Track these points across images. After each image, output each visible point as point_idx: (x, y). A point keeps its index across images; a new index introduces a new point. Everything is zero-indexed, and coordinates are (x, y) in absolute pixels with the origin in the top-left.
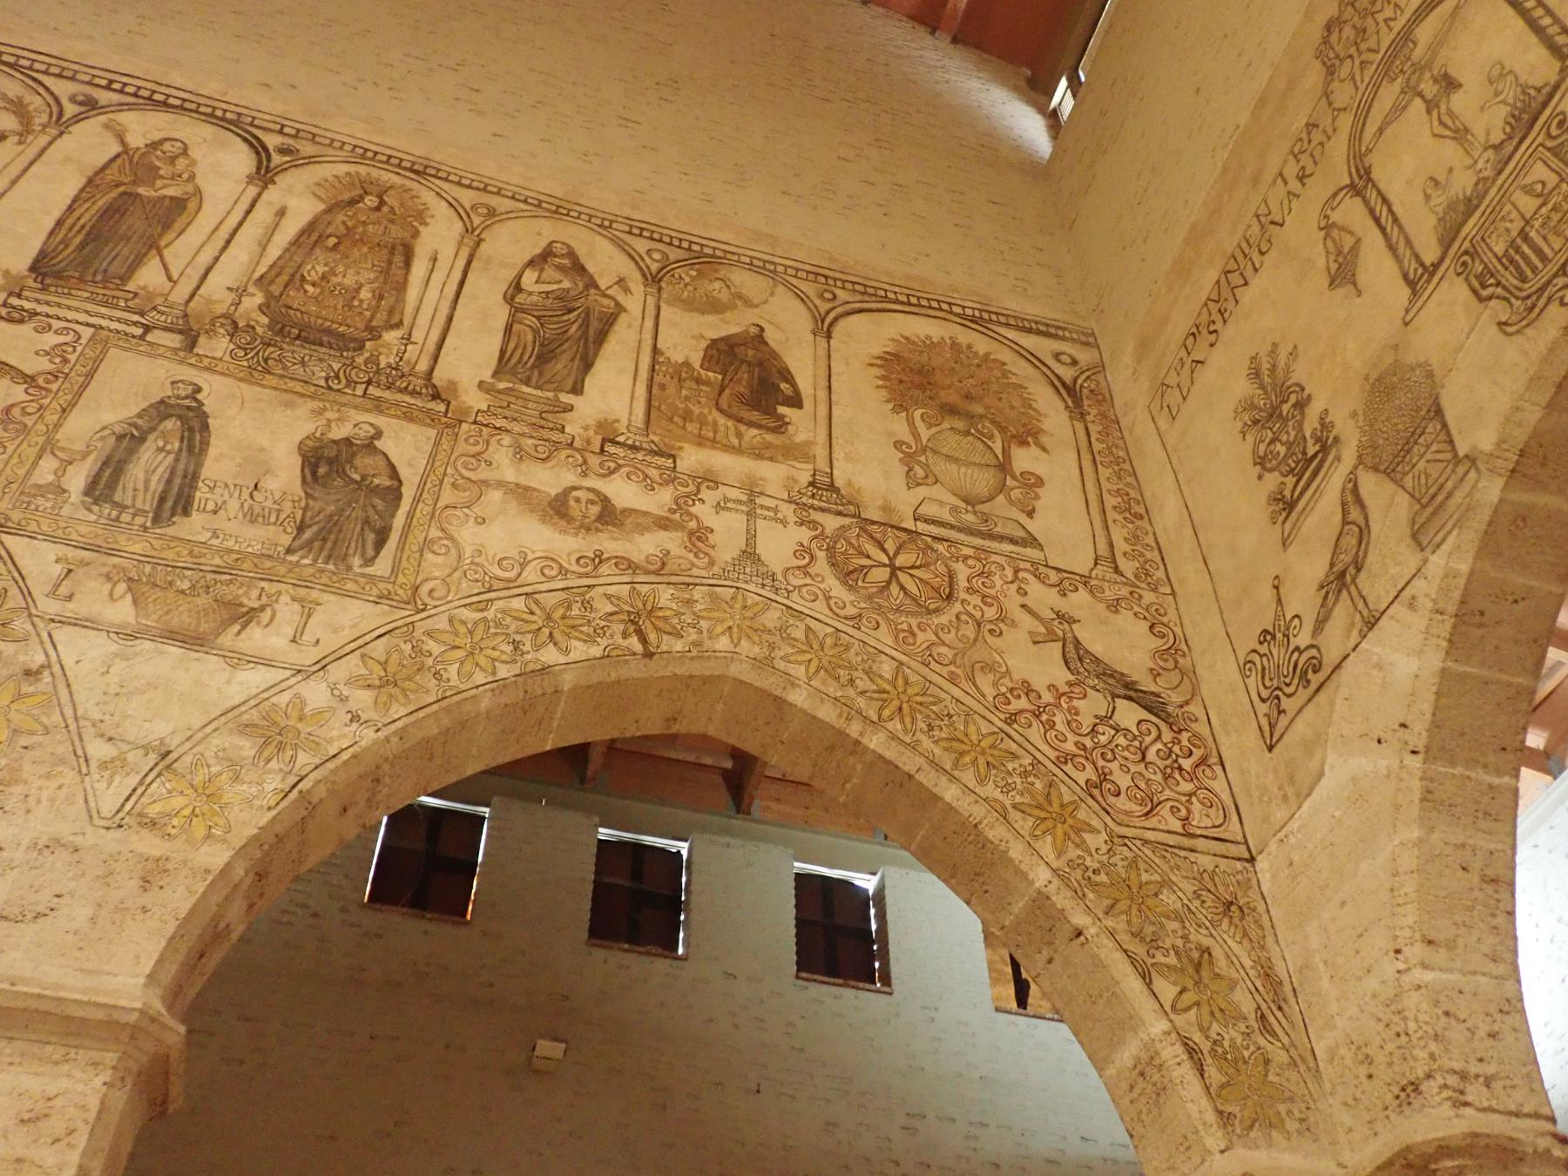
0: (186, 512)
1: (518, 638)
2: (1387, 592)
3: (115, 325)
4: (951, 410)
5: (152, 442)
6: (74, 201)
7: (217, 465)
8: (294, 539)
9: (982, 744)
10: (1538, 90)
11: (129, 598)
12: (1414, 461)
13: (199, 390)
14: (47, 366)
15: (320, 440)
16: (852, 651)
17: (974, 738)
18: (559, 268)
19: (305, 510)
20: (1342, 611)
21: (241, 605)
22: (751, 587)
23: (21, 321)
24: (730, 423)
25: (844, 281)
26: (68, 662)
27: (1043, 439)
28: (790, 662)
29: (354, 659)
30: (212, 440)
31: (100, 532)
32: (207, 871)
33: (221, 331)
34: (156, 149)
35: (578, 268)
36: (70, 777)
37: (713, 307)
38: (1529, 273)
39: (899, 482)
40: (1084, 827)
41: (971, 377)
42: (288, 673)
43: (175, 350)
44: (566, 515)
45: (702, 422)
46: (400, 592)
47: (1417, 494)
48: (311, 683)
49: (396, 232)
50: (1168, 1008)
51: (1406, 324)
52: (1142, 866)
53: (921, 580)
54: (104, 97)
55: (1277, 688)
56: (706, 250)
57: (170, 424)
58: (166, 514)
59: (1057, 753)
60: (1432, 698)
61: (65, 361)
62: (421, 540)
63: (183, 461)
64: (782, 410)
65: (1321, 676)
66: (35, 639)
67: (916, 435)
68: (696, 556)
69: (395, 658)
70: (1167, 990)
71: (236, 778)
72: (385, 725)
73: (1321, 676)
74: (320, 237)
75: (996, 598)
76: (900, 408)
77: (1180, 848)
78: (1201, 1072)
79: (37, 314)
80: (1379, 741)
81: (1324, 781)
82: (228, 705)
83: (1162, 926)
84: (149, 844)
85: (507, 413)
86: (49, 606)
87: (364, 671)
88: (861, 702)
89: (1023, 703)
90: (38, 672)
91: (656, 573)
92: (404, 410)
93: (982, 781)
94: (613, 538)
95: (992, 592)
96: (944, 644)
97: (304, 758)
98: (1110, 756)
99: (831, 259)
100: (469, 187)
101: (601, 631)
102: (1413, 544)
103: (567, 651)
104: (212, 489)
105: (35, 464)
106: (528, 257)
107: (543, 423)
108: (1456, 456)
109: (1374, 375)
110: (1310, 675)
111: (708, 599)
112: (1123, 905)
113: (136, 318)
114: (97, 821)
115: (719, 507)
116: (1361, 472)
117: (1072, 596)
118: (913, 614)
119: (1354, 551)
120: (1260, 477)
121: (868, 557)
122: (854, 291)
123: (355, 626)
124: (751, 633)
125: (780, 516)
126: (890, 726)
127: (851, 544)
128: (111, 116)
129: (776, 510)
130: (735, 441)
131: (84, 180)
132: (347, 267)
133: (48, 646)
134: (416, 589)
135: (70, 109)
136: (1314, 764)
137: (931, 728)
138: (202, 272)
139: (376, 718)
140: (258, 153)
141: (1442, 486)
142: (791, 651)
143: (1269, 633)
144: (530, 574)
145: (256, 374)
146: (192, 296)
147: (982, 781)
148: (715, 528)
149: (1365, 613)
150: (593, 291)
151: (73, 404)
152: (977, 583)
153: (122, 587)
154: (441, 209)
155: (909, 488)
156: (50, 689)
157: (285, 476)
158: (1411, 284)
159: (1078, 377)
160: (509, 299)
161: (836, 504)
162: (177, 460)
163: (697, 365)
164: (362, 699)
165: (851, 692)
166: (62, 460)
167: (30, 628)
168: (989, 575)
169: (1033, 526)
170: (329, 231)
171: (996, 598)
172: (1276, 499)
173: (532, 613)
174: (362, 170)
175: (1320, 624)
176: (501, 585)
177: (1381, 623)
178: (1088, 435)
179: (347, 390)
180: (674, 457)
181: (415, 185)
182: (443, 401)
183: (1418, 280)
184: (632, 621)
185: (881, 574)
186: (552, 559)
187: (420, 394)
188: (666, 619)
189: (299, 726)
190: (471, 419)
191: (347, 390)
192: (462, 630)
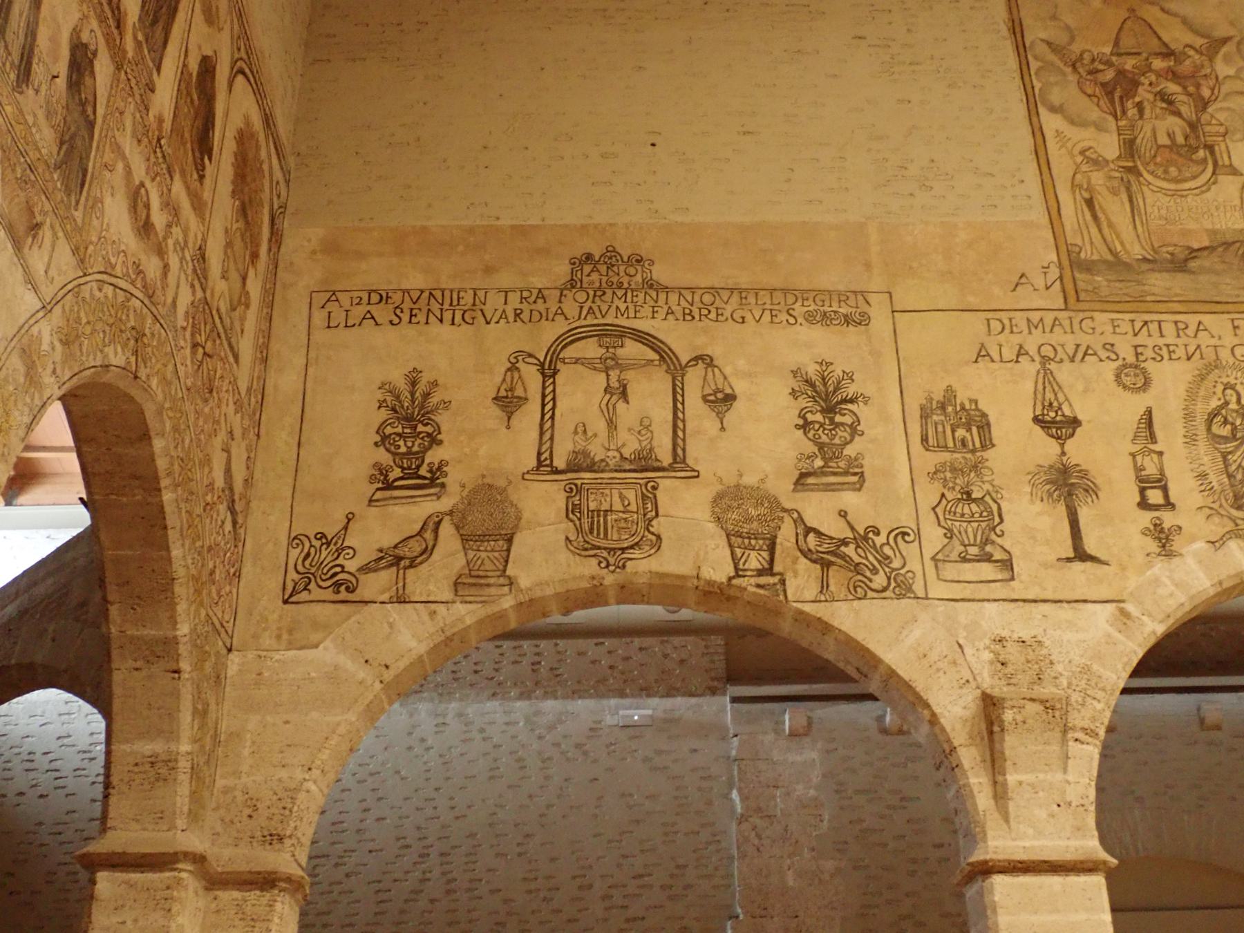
2: (421, 594)
10: (657, 460)
12: (481, 548)
20: (385, 577)
38: (595, 532)
47: (471, 565)
51: (523, 479)
55: (313, 574)
60: (408, 663)
65: (351, 597)
73: (351, 597)
80: (366, 661)
81: (314, 651)
102: (453, 588)
108: (505, 571)
109: (488, 480)
110: (343, 588)
116: (447, 518)
119: (415, 554)
120: (376, 444)
136: (315, 637)
141: (487, 577)
143: (326, 538)
149: (401, 592)
158: (540, 463)
172: (380, 470)
175: (365, 569)
177: (407, 606)
183: (544, 465)
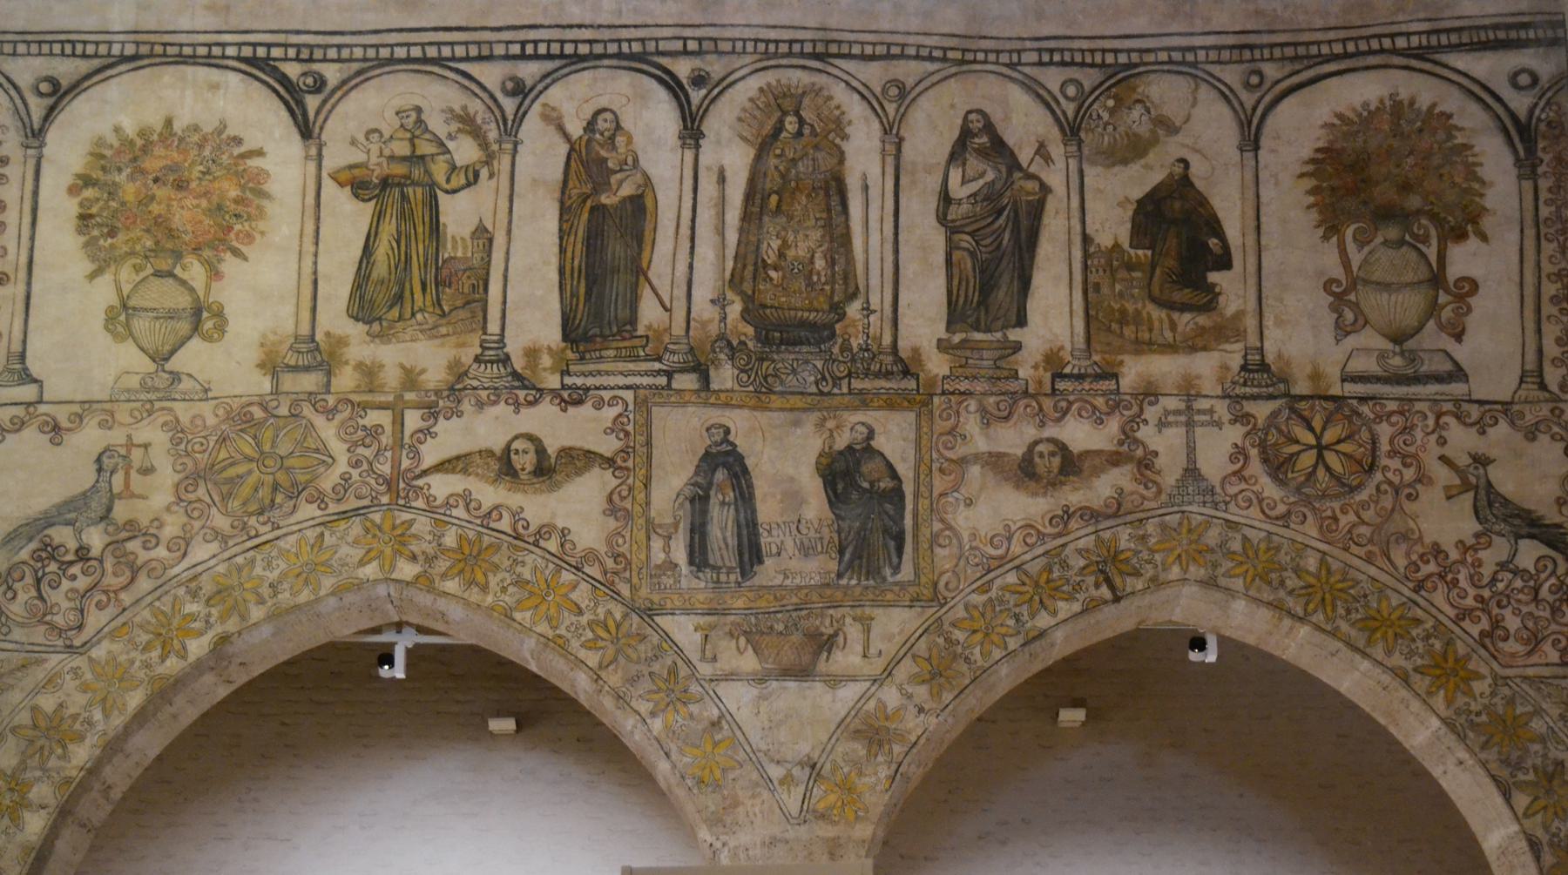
0: (761, 562)
1: (1017, 610)
3: (646, 381)
4: (1386, 214)
5: (715, 499)
6: (561, 238)
7: (767, 510)
8: (840, 563)
9: (1393, 617)
11: (750, 647)
13: (727, 431)
14: (617, 445)
15: (830, 454)
16: (1283, 551)
17: (1385, 614)
18: (982, 153)
19: (839, 532)
21: (822, 634)
22: (1194, 508)
23: (579, 402)
24: (1163, 314)
25: (1272, 46)
26: (733, 710)
27: (1487, 223)
28: (1230, 577)
29: (907, 661)
30: (755, 482)
31: (712, 596)
32: (864, 841)
33: (722, 356)
34: (593, 131)
35: (998, 148)
36: (766, 794)
37: (1133, 150)
39: (1328, 335)
40: (1478, 676)
41: (1411, 153)
42: (868, 684)
43: (696, 392)
44: (1034, 474)
45: (1137, 319)
46: (925, 592)
48: (885, 688)
49: (826, 161)
50: (1520, 814)
52: (1518, 701)
53: (1344, 454)
54: (529, 71)
56: (1123, 59)
57: (720, 475)
58: (748, 567)
59: (1456, 611)
61: (627, 434)
62: (929, 536)
63: (742, 510)
64: (1214, 277)
66: (706, 696)
67: (1346, 263)
68: (1147, 488)
69: (935, 651)
70: (1522, 800)
71: (860, 774)
72: (942, 711)
74: (762, 199)
75: (1415, 456)
76: (1331, 227)
77: (1556, 677)
78: (1538, 858)
79: (588, 389)
82: (838, 719)
83: (1527, 751)
84: (825, 831)
85: (968, 372)
86: (705, 669)
87: (917, 670)
88: (1290, 602)
89: (1432, 567)
90: (719, 722)
91: (1115, 515)
92: (884, 397)
93: (1389, 652)
94: (1076, 489)
95: (1412, 449)
96: (1364, 522)
97: (897, 749)
98: (1505, 602)
99: (1258, 13)
100: (873, 58)
101: (1078, 587)
103: (1054, 613)
104: (769, 532)
105: (648, 547)
106: (947, 149)
107: (998, 373)
111: (1159, 530)
112: (1496, 739)
113: (657, 366)
114: (792, 821)
115: (1162, 425)
117: (1491, 431)
118: (1337, 496)
121: (1297, 442)
122: (1283, 59)
123: (902, 631)
124: (1197, 556)
125: (1216, 417)
126: (1314, 619)
127: (1280, 431)
128: (542, 99)
129: (1211, 411)
130: (1168, 335)
131: (556, 205)
132: (796, 232)
133: (717, 700)
134: (935, 585)
135: (509, 105)
137: (1348, 611)
138: (685, 288)
139: (934, 706)
140: (676, 97)
142: (1230, 564)
144: (1016, 548)
145: (763, 398)
146: (688, 323)
147: (1389, 653)
148: (1160, 449)
150: (1017, 175)
151: (648, 478)
152: (1399, 441)
153: (742, 640)
154: (855, 109)
155: (1338, 341)
156: (731, 734)
157: (815, 506)
159: (1536, 104)
160: (942, 218)
161: (1267, 386)
162: (737, 510)
163: (1126, 246)
164: (921, 692)
165: (1282, 594)
166: (664, 537)
167: (701, 689)
168: (1413, 427)
169: (1461, 353)
170: (768, 186)
171: (1415, 456)
173: (1024, 584)
174: (770, 77)
176: (996, 563)
178: (1536, 199)
179: (836, 391)
180: (1115, 376)
181: (821, 80)
182: (912, 375)
184: (1102, 572)
185: (1308, 459)
186: (1032, 526)
187: (892, 373)
188: (1127, 560)
189: (887, 724)
190: (939, 391)
191: (836, 391)
192: (976, 614)
